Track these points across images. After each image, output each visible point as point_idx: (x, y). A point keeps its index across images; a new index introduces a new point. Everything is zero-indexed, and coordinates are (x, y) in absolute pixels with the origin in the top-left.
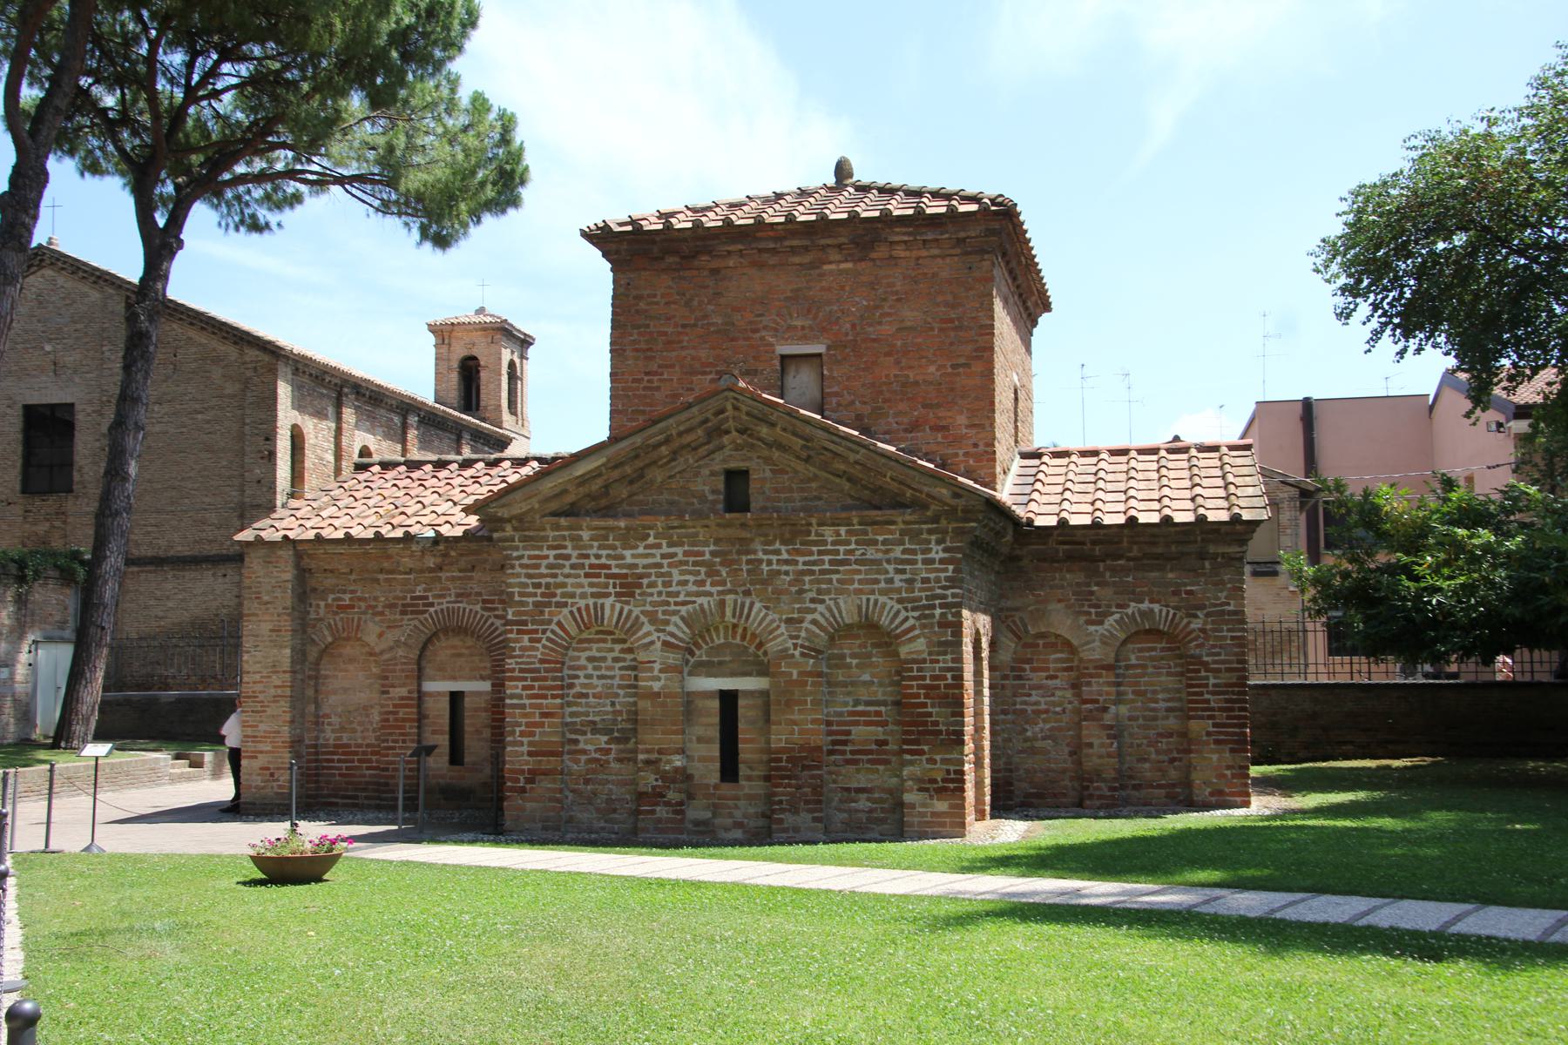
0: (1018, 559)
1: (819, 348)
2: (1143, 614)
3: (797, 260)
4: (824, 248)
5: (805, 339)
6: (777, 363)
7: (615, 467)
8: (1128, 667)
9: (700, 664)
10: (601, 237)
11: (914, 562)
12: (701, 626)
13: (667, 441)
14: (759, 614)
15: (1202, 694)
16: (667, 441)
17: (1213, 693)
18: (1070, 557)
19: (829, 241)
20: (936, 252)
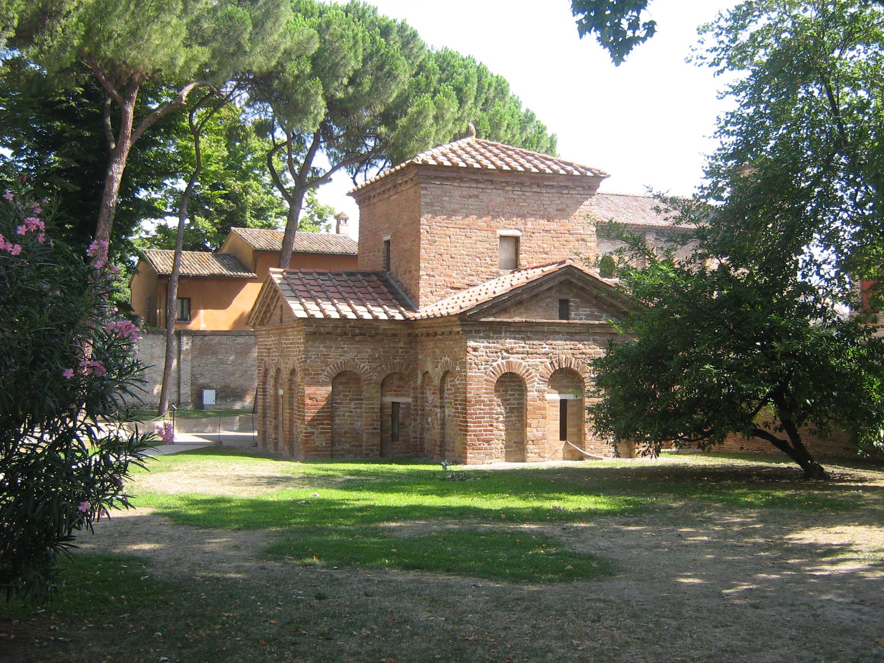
0: (417, 336)
1: (388, 238)
2: (446, 362)
3: (386, 196)
4: (389, 189)
5: (387, 233)
6: (383, 247)
7: (263, 306)
8: (448, 390)
9: (281, 384)
10: (349, 194)
11: (298, 343)
12: (278, 371)
13: (267, 296)
14: (282, 366)
15: (456, 404)
16: (267, 296)
17: (460, 404)
18: (428, 335)
19: (388, 187)
20: (409, 186)
